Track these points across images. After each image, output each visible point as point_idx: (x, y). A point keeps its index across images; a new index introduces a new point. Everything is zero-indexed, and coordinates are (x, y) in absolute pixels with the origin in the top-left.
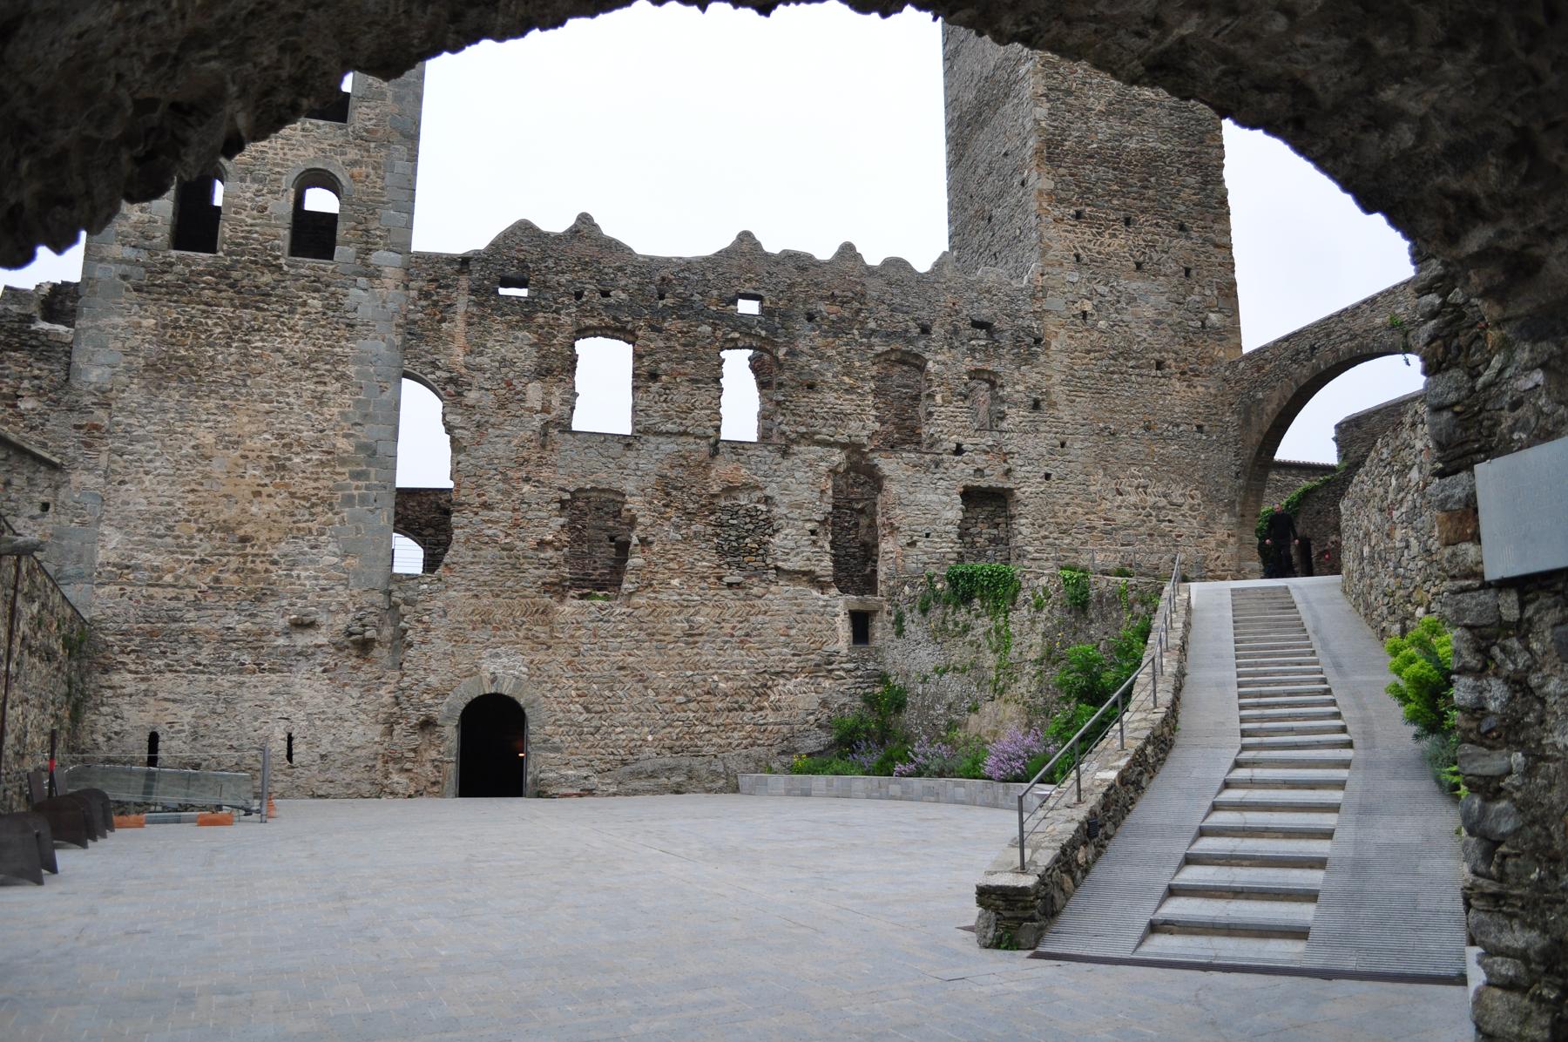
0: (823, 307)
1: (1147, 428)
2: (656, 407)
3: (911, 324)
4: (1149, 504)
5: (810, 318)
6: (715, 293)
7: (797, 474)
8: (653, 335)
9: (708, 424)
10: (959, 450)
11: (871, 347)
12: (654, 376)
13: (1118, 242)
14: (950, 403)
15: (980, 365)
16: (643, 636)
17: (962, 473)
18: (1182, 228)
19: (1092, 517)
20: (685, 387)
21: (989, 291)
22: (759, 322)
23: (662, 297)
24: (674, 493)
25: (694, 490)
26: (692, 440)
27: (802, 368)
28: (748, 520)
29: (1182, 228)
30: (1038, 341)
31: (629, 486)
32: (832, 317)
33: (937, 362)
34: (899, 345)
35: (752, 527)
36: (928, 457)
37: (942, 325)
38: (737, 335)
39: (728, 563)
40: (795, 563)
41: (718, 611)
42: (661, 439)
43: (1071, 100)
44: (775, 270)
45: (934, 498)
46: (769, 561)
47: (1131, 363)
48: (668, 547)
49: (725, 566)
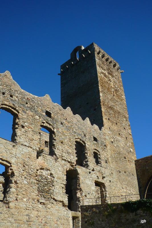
0: (64, 121)
1: (125, 172)
2: (23, 136)
3: (82, 133)
4: (128, 192)
5: (62, 124)
6: (40, 108)
7: (59, 168)
8: (23, 114)
9: (37, 146)
10: (93, 170)
11: (75, 136)
12: (23, 127)
13: (115, 127)
14: (91, 156)
15: (96, 148)
16: (13, 221)
17: (94, 176)
18: (124, 129)
19: (119, 194)
20: (31, 133)
21: (95, 130)
22: (50, 120)
23: (27, 103)
24: (26, 166)
25: (32, 167)
26: (31, 149)
27: (60, 136)
28: (46, 180)
29: (124, 129)
30: (105, 145)
31: (13, 161)
32: (66, 125)
33: (88, 144)
34: (80, 137)
35: (46, 183)
36: (88, 170)
37: (88, 136)
38: (45, 122)
39: (41, 195)
40: (59, 198)
41: (37, 212)
42: (23, 147)
43: (105, 94)
44: (54, 107)
45: (90, 182)
46: (52, 196)
47: (121, 156)
48: (23, 186)
49: (40, 196)
